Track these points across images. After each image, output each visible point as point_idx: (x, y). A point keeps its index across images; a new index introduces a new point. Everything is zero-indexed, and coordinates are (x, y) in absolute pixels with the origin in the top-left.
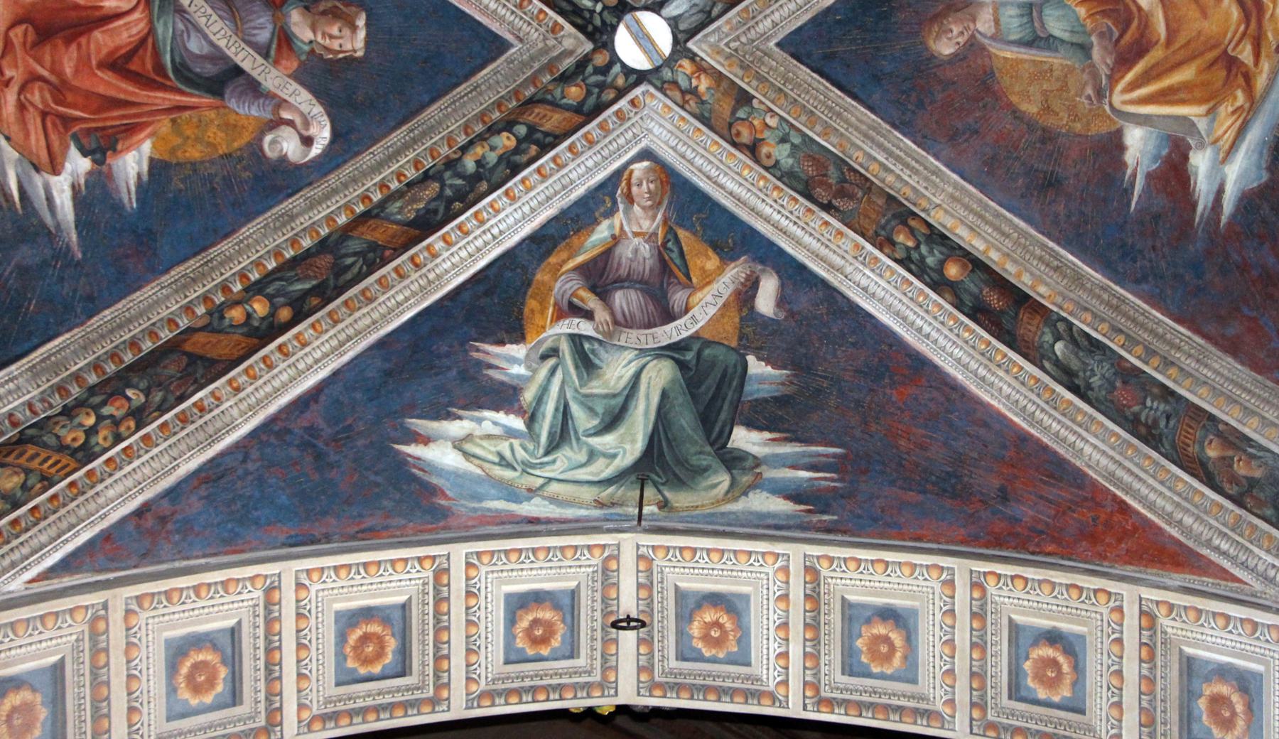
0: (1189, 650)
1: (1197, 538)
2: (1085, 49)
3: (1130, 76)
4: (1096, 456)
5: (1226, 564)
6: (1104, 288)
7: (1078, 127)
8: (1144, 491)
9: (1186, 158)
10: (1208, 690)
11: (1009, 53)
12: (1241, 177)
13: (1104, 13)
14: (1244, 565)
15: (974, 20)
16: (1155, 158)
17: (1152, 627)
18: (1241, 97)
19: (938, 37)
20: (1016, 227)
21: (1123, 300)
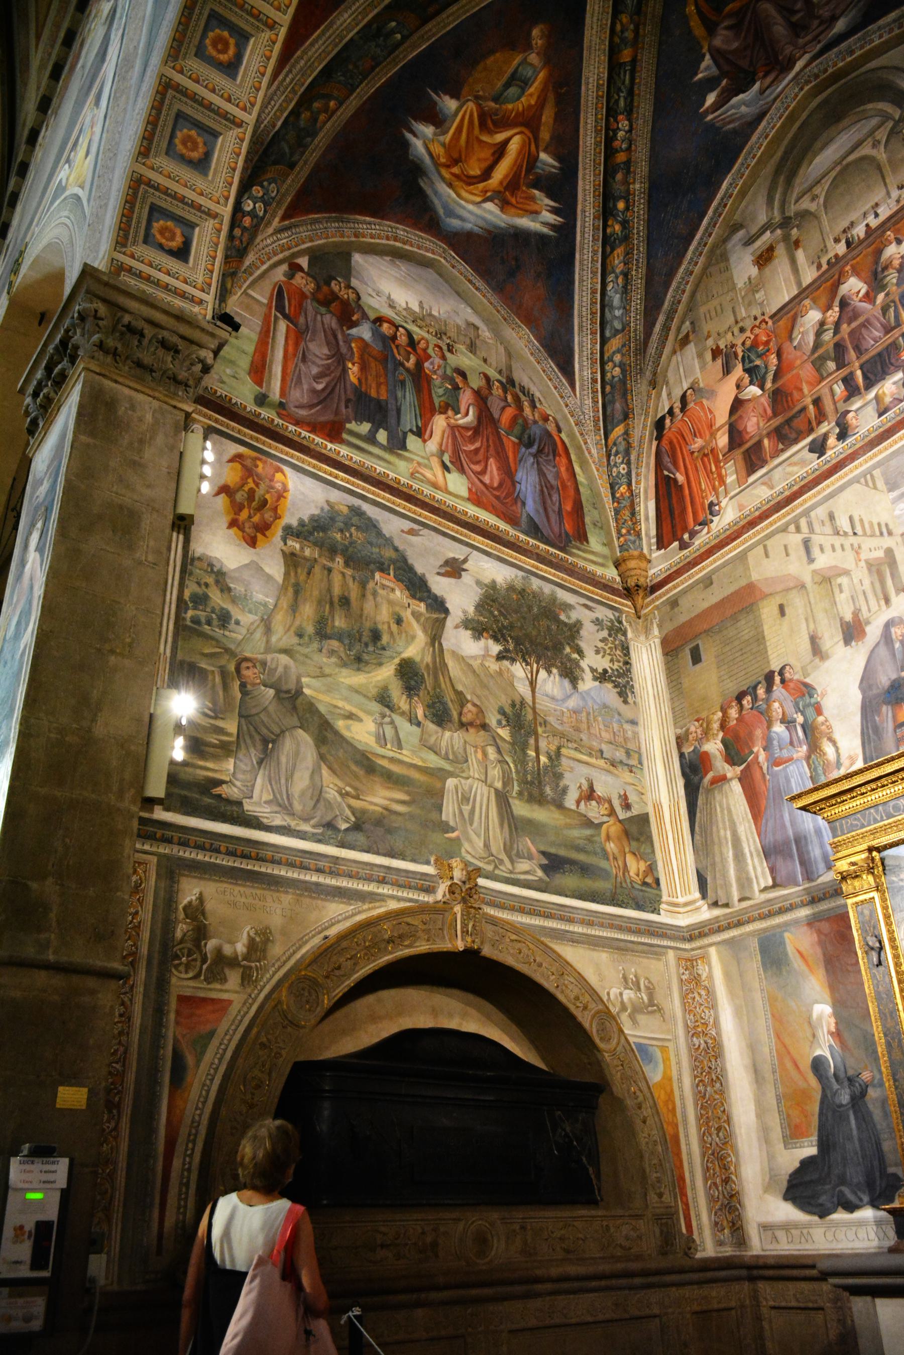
0: (252, 41)
1: (294, 66)
2: (496, 99)
3: (475, 114)
4: (342, 19)
5: (280, 78)
6: (405, 57)
7: (471, 80)
8: (320, 42)
9: (434, 125)
10: (232, 41)
11: (516, 62)
12: (416, 147)
13: (503, 117)
14: (278, 88)
15: (538, 54)
16: (441, 110)
17: (266, 24)
18: (443, 160)
19: (542, 30)
20: (449, 24)
21: (397, 65)
